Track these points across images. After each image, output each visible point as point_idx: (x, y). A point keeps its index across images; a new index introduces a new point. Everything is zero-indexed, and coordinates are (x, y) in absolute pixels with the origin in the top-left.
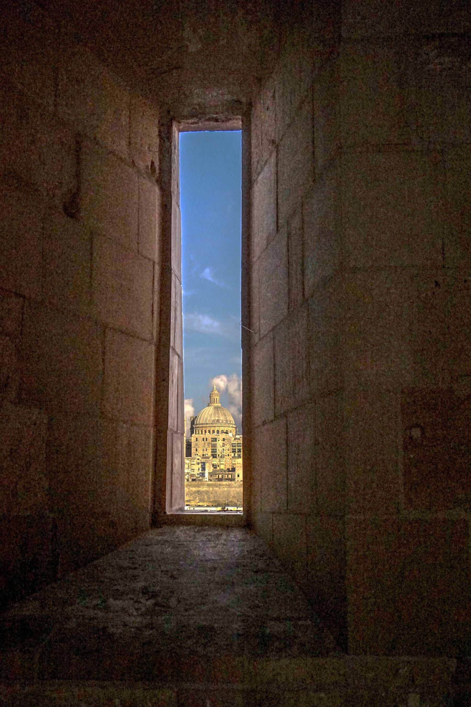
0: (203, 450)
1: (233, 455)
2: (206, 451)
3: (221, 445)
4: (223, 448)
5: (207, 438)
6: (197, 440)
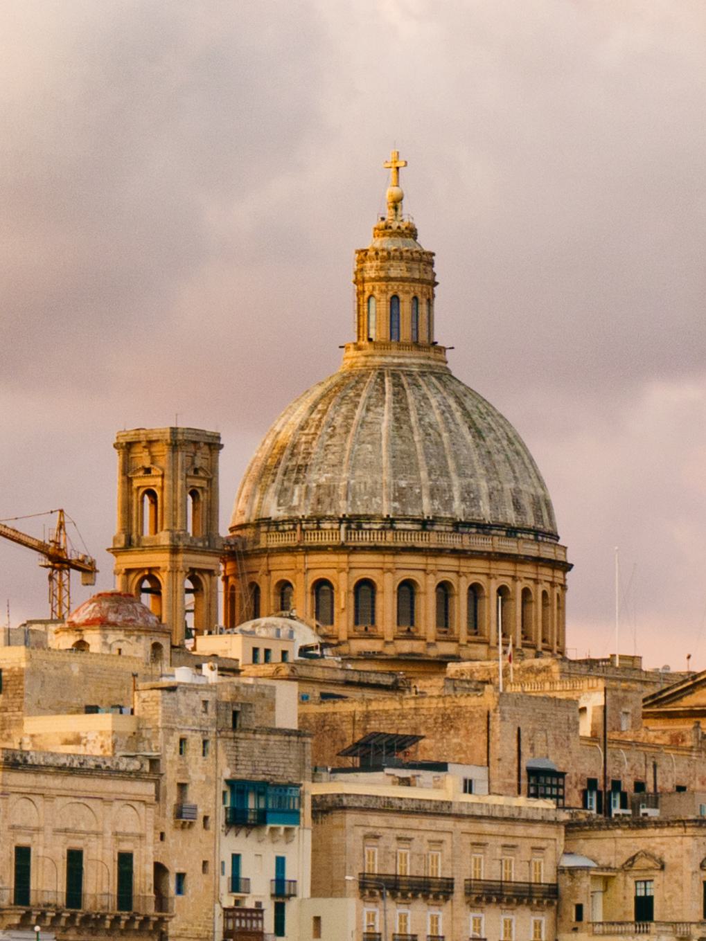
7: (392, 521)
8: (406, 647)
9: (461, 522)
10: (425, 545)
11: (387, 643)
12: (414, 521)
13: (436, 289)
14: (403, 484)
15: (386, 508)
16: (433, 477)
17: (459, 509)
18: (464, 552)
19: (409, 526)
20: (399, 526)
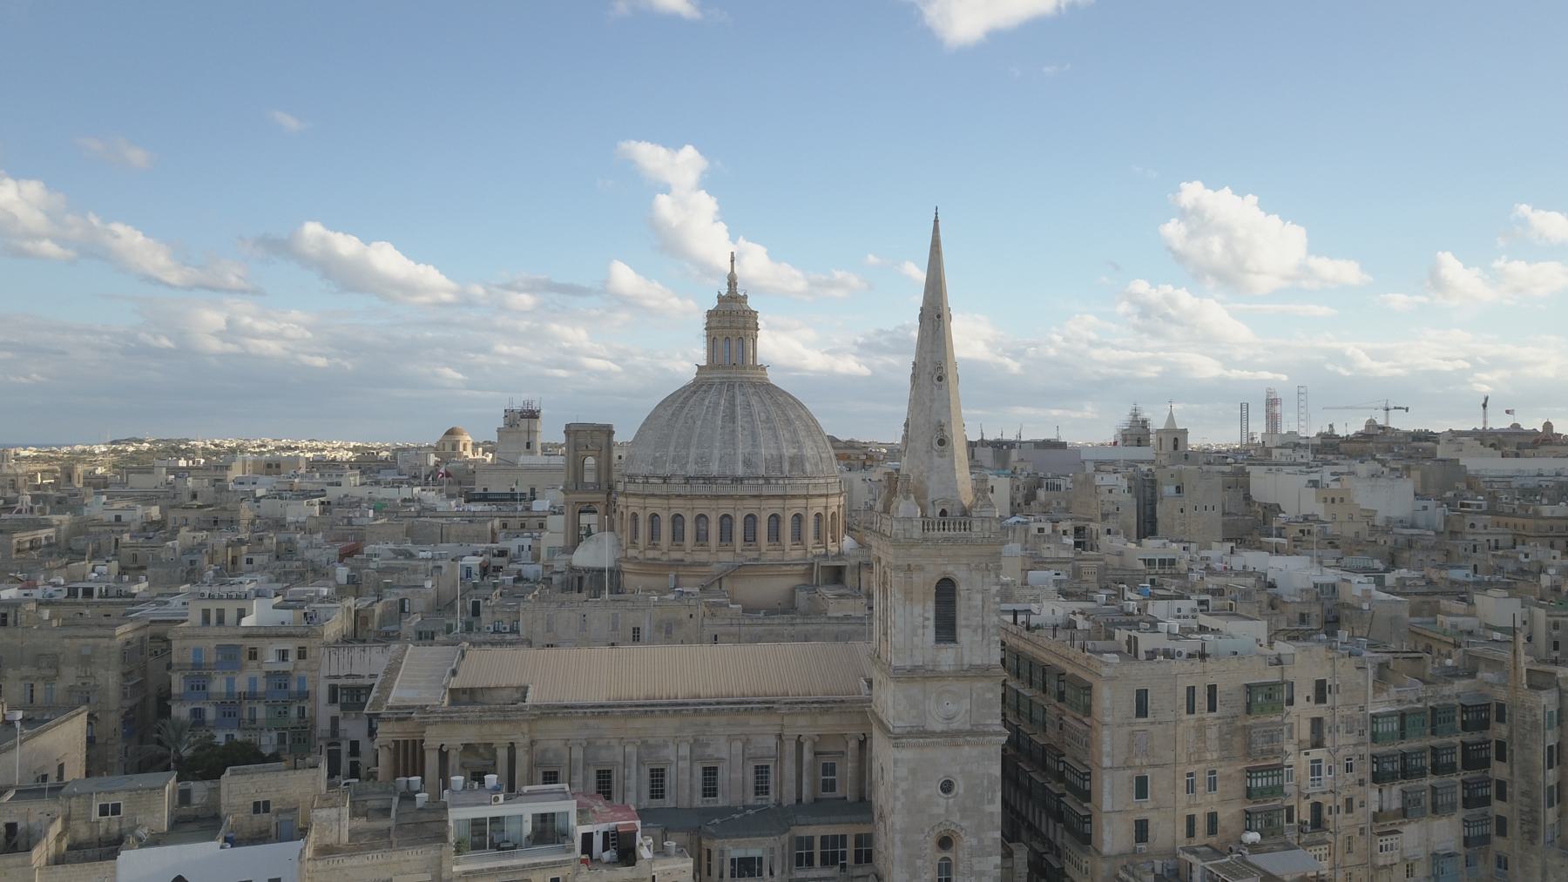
0: (1190, 788)
1: (1372, 797)
2: (1212, 785)
3: (1305, 732)
4: (1316, 754)
5: (1212, 690)
6: (1142, 710)
7: (647, 478)
8: (651, 554)
9: (690, 477)
10: (661, 493)
11: (640, 552)
12: (659, 477)
13: (758, 332)
14: (658, 455)
15: (645, 469)
16: (678, 450)
17: (691, 470)
18: (686, 496)
19: (656, 481)
20: (651, 480)
